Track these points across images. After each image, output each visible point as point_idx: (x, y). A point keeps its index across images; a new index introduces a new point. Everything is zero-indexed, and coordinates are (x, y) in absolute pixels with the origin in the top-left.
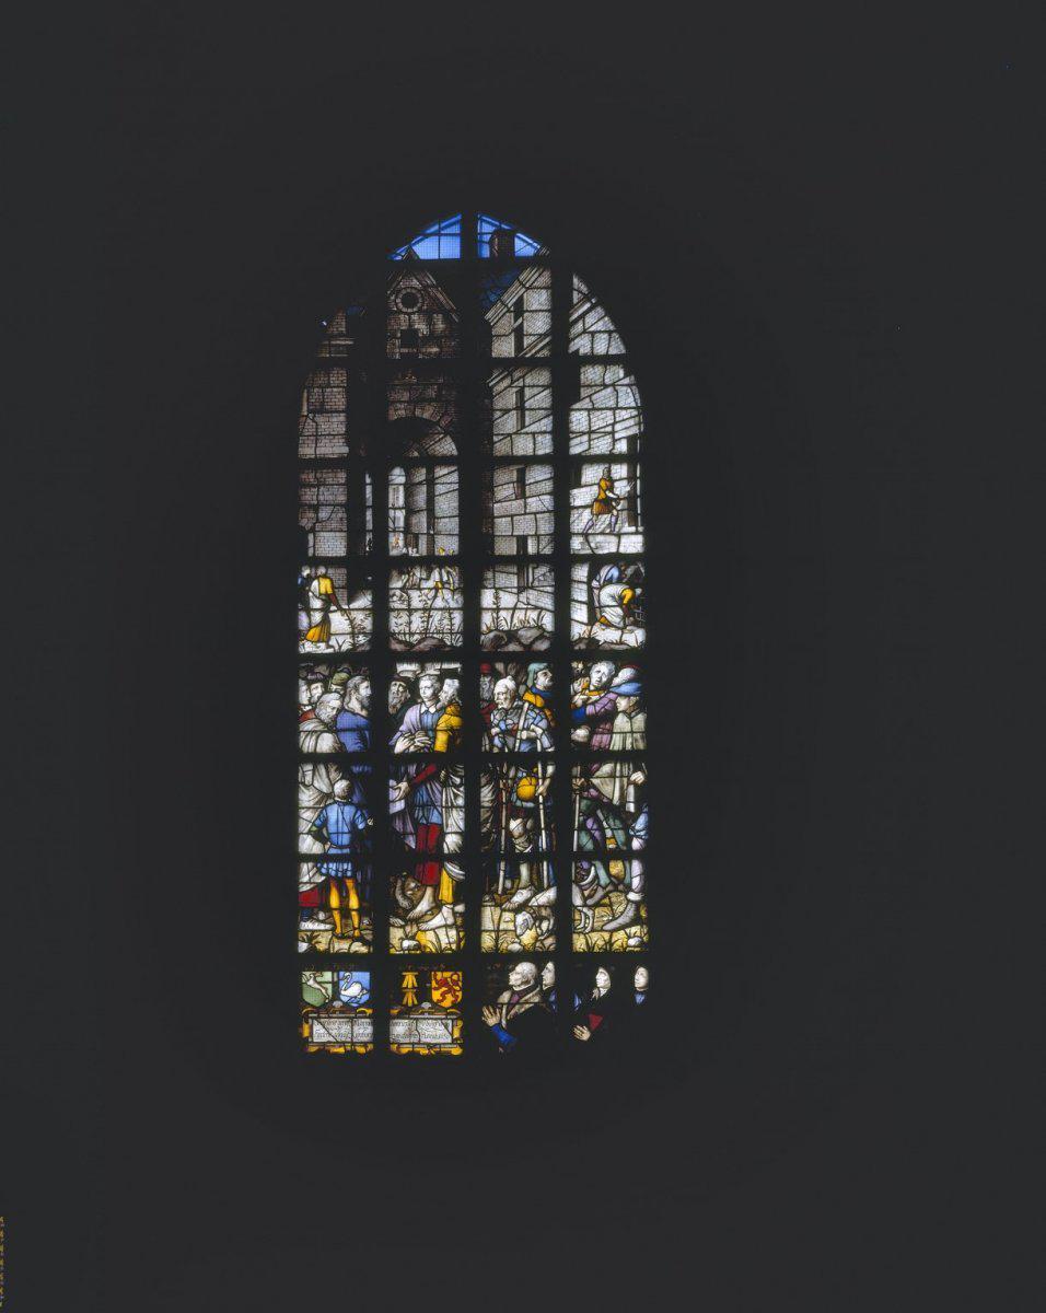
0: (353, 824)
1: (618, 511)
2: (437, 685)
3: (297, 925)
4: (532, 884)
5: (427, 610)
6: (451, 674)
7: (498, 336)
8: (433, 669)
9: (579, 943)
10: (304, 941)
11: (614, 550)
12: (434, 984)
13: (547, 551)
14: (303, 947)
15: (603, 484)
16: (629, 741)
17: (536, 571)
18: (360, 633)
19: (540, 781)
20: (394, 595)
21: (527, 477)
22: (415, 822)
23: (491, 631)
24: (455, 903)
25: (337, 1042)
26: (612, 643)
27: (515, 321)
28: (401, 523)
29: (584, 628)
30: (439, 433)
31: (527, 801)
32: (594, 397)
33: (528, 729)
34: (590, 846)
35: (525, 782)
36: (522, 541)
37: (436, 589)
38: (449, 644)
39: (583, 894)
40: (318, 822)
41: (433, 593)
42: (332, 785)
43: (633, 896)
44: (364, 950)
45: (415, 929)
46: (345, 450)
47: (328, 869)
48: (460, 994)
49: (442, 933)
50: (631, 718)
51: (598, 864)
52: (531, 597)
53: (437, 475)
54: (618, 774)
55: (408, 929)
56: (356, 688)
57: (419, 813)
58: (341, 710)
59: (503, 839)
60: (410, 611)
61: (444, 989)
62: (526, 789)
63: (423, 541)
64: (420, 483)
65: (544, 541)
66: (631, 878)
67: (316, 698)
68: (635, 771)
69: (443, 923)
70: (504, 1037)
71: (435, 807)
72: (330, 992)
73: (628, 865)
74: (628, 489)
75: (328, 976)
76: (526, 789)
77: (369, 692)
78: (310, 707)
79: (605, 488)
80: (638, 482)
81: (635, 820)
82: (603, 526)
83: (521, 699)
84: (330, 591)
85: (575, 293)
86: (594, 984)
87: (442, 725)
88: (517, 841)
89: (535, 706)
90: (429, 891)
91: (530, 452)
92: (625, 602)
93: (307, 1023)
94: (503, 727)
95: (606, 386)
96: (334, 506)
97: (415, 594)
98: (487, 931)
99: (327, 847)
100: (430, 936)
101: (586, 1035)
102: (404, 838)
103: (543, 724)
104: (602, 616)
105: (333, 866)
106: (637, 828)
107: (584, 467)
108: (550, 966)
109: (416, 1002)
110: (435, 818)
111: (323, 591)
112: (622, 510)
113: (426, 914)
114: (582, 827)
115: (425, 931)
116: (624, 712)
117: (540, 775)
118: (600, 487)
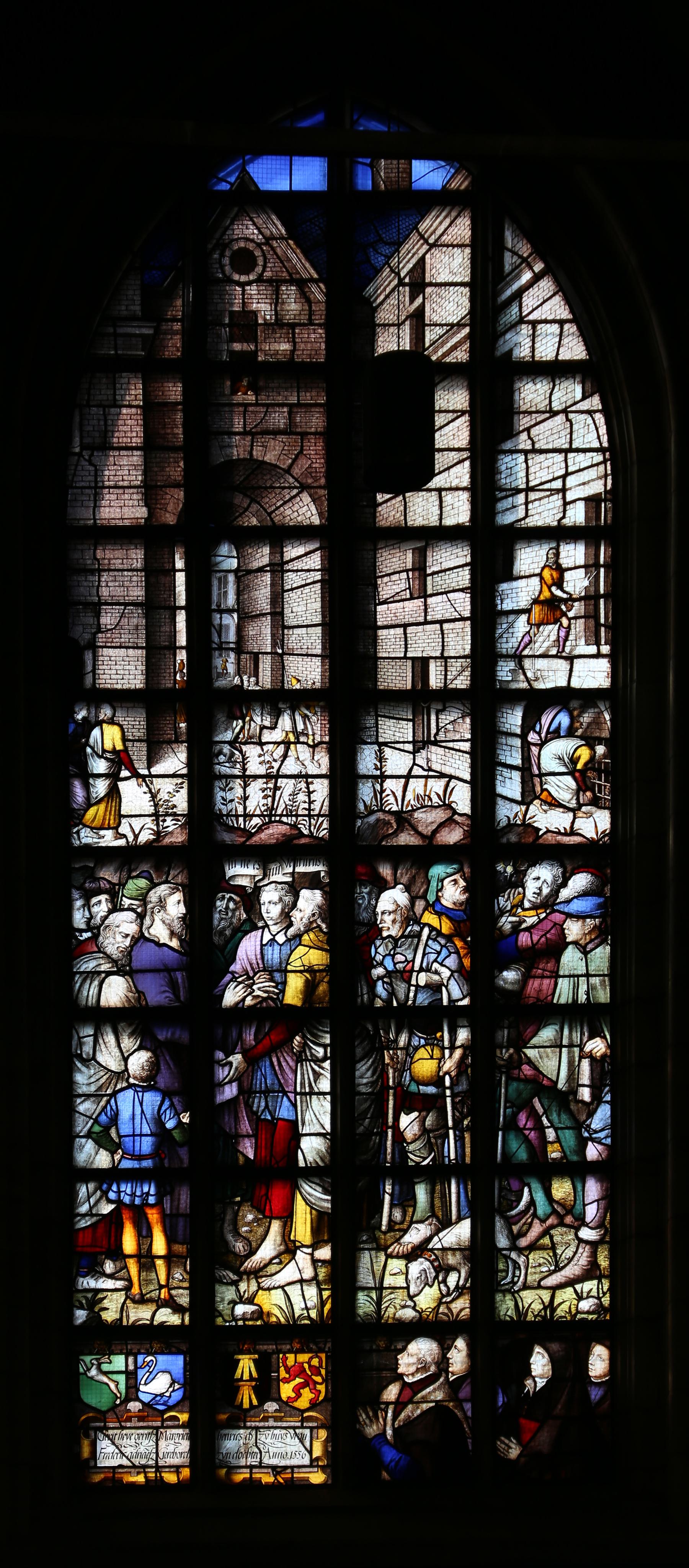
0: (159, 1121)
1: (569, 619)
2: (288, 899)
3: (74, 1282)
4: (434, 1215)
5: (272, 777)
6: (312, 881)
7: (385, 325)
8: (282, 874)
9: (506, 1307)
10: (81, 1307)
11: (563, 683)
12: (283, 1374)
13: (462, 682)
14: (81, 1315)
15: (547, 574)
16: (583, 988)
17: (442, 717)
18: (167, 814)
19: (447, 1052)
20: (220, 752)
21: (429, 560)
22: (255, 1118)
23: (372, 812)
24: (315, 1246)
25: (134, 1466)
26: (559, 833)
27: (412, 301)
28: (232, 636)
29: (516, 808)
30: (291, 488)
31: (426, 1084)
32: (534, 432)
33: (428, 970)
34: (522, 1155)
35: (422, 1053)
36: (421, 665)
37: (287, 744)
38: (306, 832)
39: (510, 1231)
40: (103, 1118)
41: (281, 750)
42: (126, 1060)
43: (586, 1234)
44: (174, 1320)
45: (254, 1286)
46: (142, 512)
47: (119, 1192)
48: (322, 1388)
49: (294, 1292)
50: (585, 953)
51: (536, 1186)
52: (433, 757)
53: (287, 557)
54: (565, 1042)
55: (243, 1286)
56: (162, 903)
57: (259, 1103)
58: (140, 939)
59: (389, 1143)
60: (246, 779)
61: (298, 1380)
62: (424, 1066)
63: (266, 665)
64: (261, 570)
65: (455, 667)
66: (584, 1205)
67: (98, 920)
68: (591, 1038)
69: (297, 1277)
70: (389, 1455)
71: (285, 1093)
72: (122, 1387)
73: (579, 1188)
74: (586, 583)
75: (119, 1362)
76: (424, 1066)
77: (182, 909)
78: (89, 934)
79: (550, 582)
80: (602, 570)
81: (591, 1114)
82: (546, 644)
83: (417, 921)
84: (119, 746)
85: (507, 255)
86: (527, 1371)
87: (296, 962)
88: (411, 1148)
89: (439, 933)
90: (276, 1226)
91: (434, 521)
92: (579, 766)
93: (87, 1436)
94: (390, 967)
95: (554, 414)
96: (126, 605)
97: (252, 751)
98: (364, 1289)
99: (117, 1157)
100: (277, 1297)
101: (514, 1452)
102: (238, 1143)
103: (452, 961)
104: (543, 790)
105: (126, 1188)
106: (593, 1126)
107: (518, 547)
108: (460, 1343)
109: (255, 1402)
110: (285, 1112)
111: (108, 746)
112: (575, 618)
113: (270, 1262)
114: (511, 1125)
115: (269, 1289)
116: (575, 943)
117: (446, 1044)
118: (542, 579)
